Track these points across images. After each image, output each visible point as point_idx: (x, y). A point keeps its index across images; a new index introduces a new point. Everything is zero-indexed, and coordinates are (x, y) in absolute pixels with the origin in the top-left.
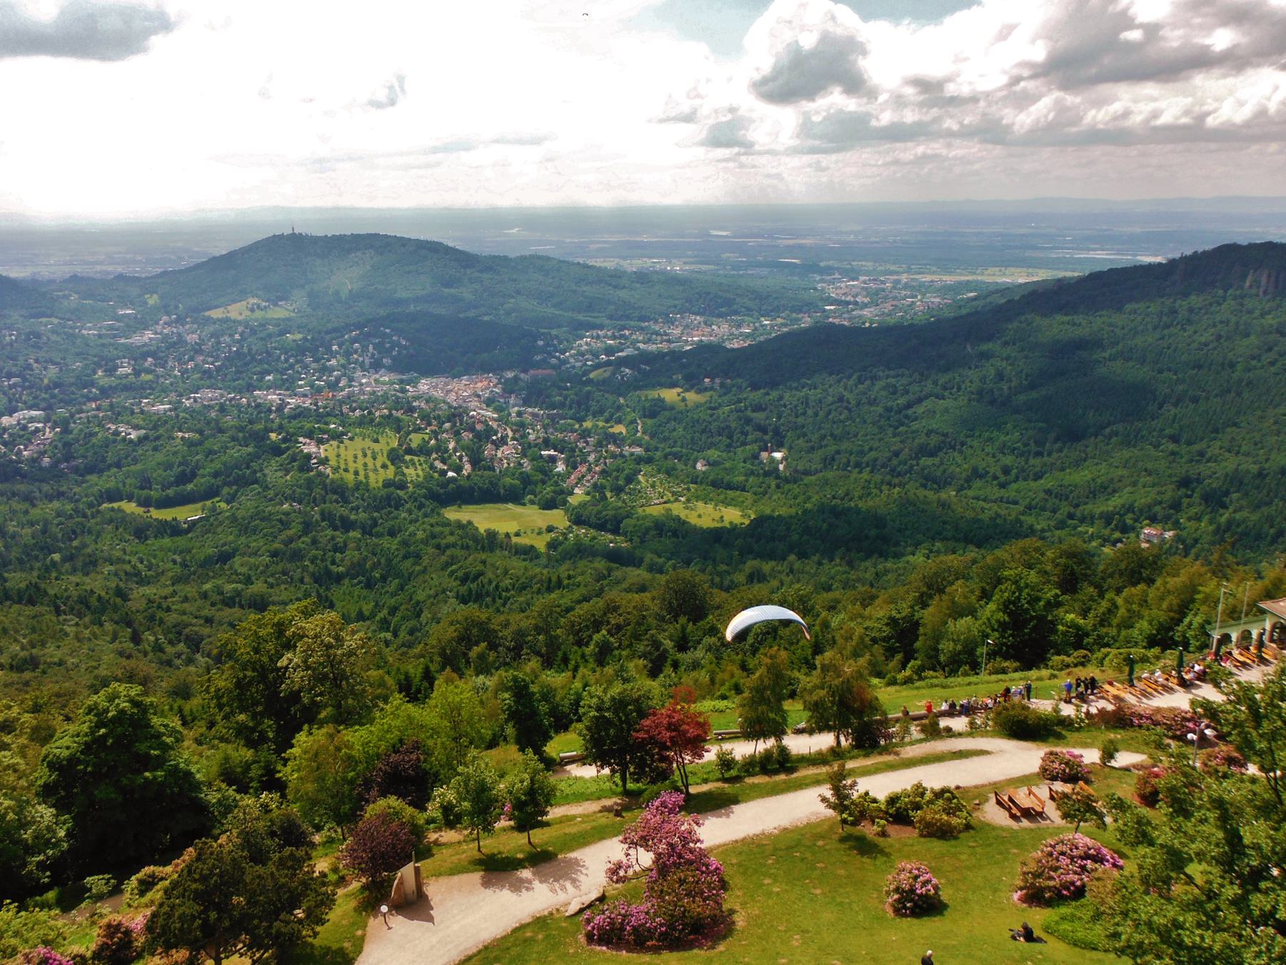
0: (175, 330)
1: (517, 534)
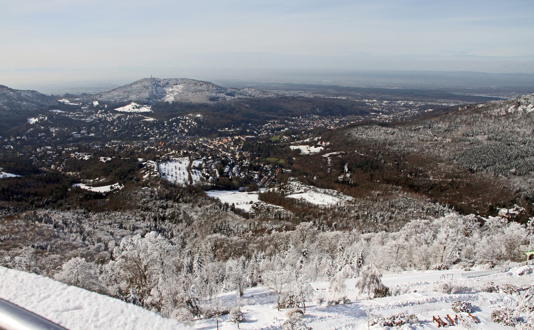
0: (103, 116)
1: (237, 204)
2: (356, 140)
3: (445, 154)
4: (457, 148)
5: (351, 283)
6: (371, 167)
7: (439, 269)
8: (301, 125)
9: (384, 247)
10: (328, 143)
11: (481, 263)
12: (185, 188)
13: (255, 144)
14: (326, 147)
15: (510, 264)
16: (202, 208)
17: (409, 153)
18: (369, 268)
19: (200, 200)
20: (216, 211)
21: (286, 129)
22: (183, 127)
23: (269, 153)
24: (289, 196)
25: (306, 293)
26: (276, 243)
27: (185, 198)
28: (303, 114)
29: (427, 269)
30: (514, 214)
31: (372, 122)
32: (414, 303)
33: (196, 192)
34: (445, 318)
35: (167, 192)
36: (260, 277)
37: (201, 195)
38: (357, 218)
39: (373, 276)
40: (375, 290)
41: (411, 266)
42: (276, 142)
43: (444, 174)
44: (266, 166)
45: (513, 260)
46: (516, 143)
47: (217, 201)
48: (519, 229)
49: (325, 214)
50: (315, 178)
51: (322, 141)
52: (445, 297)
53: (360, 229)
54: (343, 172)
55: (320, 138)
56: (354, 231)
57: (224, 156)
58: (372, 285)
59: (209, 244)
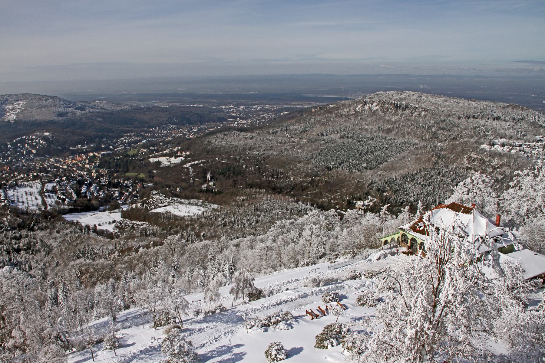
1: (99, 225)
2: (216, 148)
3: (303, 155)
4: (314, 147)
5: (225, 290)
6: (234, 173)
8: (159, 136)
9: (254, 250)
10: (188, 153)
11: (344, 254)
12: (39, 214)
13: (112, 160)
14: (186, 157)
15: (369, 251)
16: (61, 233)
17: (269, 157)
18: (240, 274)
19: (58, 225)
20: (77, 235)
21: (144, 141)
22: (30, 147)
23: (128, 168)
24: (153, 211)
25: (181, 307)
26: (145, 261)
27: (40, 225)
28: (160, 125)
30: (369, 205)
31: (230, 128)
32: (287, 301)
33: (53, 217)
35: (19, 220)
36: (132, 298)
37: (58, 220)
38: (225, 225)
39: (246, 281)
40: (249, 294)
41: (280, 266)
42: (134, 156)
43: (303, 174)
44: (126, 182)
45: (371, 247)
46: (365, 140)
47: (78, 223)
48: (373, 218)
49: (192, 225)
50: (178, 189)
51: (181, 150)
53: (229, 236)
54: (206, 181)
55: (180, 148)
56: (223, 238)
57: (79, 176)
58: (246, 289)
59: (73, 271)
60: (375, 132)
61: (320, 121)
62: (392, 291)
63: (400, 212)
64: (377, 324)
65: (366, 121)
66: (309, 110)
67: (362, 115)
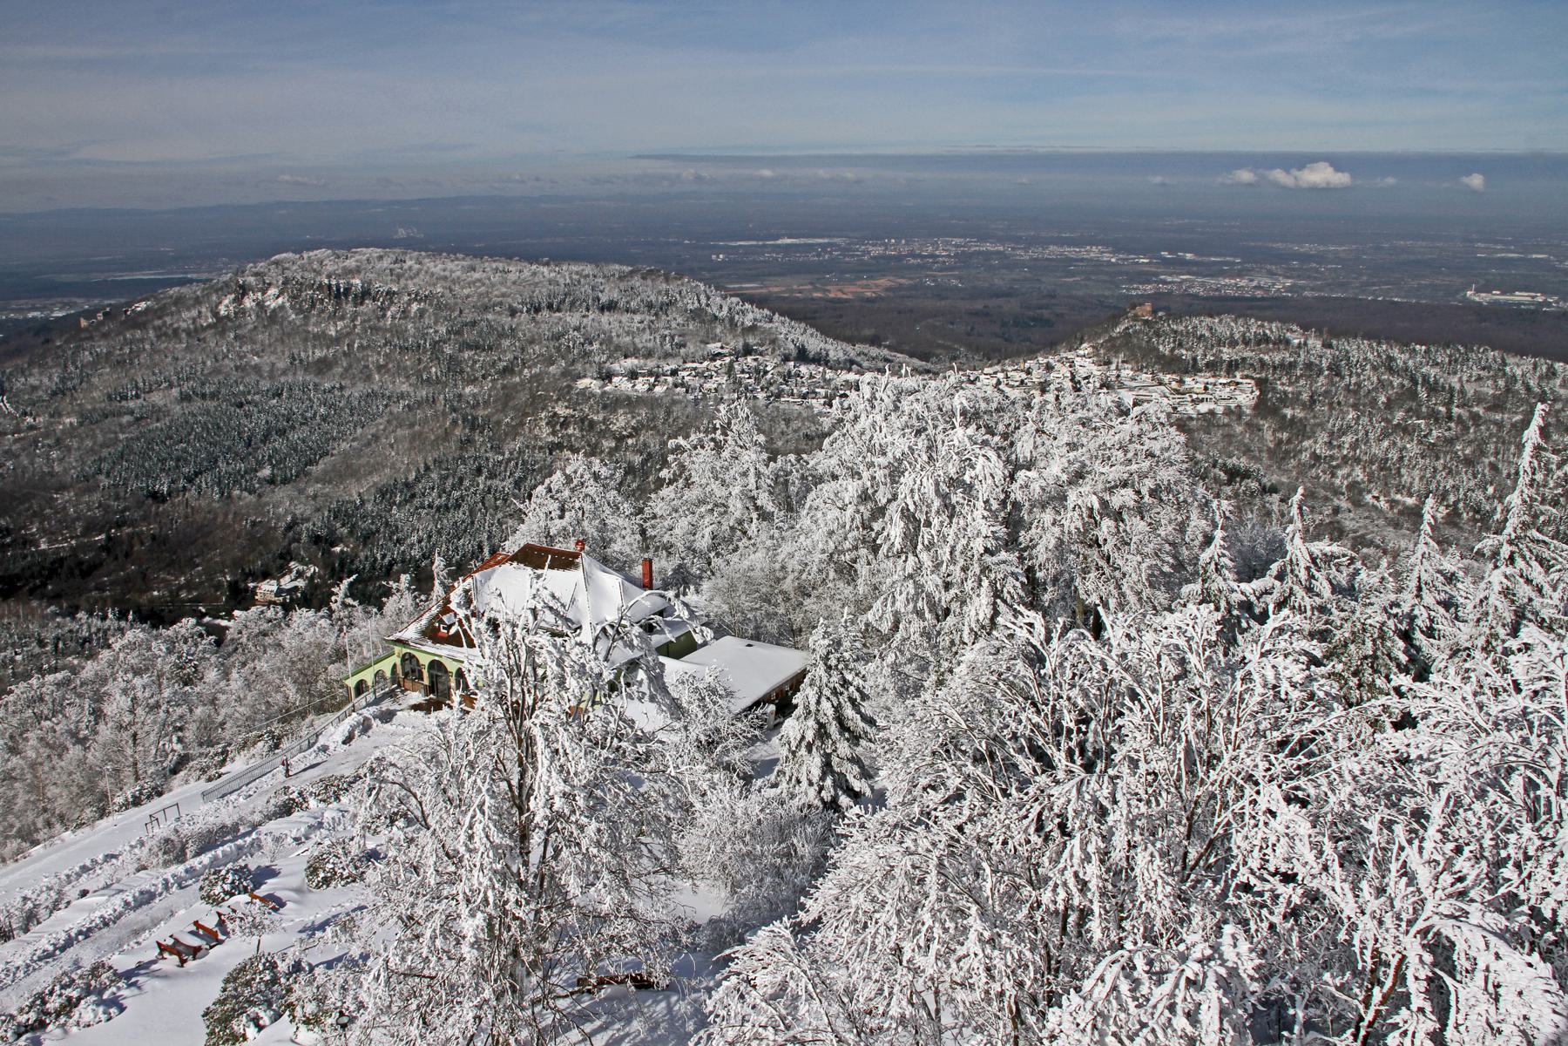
3: (68, 465)
4: (100, 438)
7: (137, 802)
11: (244, 745)
15: (316, 723)
29: (101, 817)
30: (296, 589)
34: (192, 933)
45: (321, 710)
46: (257, 398)
48: (313, 624)
52: (174, 876)
60: (284, 373)
61: (109, 354)
62: (401, 823)
63: (388, 593)
64: (376, 926)
65: (254, 342)
66: (68, 326)
67: (239, 327)
